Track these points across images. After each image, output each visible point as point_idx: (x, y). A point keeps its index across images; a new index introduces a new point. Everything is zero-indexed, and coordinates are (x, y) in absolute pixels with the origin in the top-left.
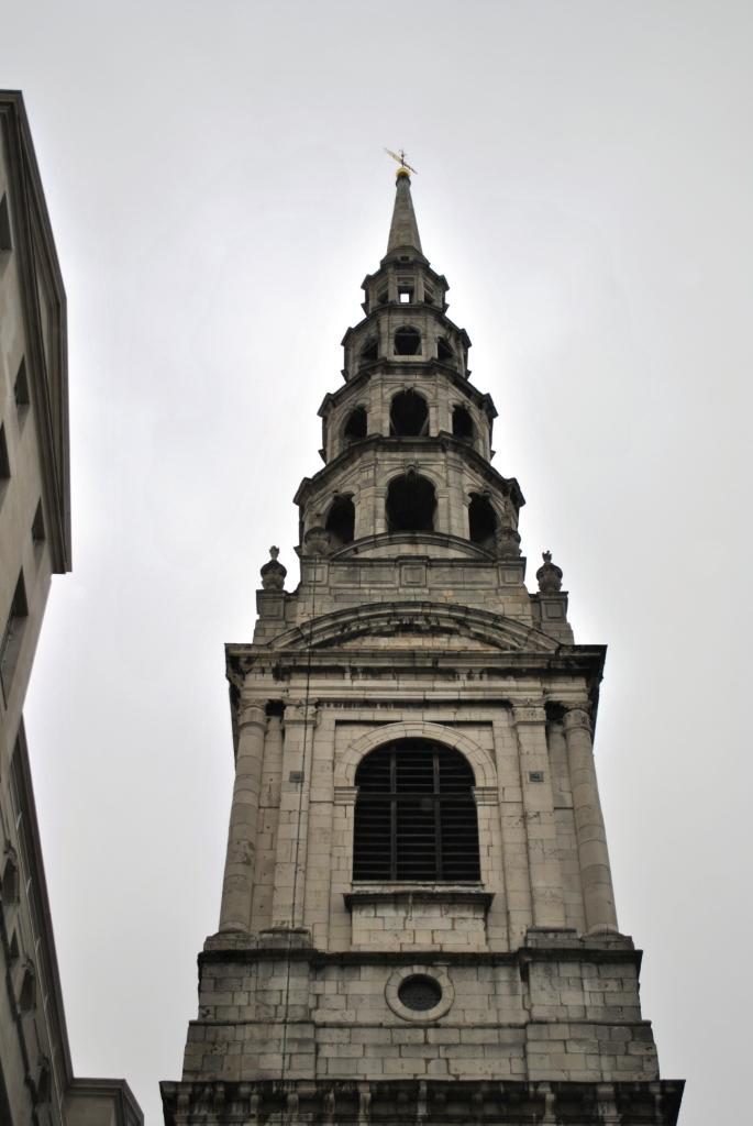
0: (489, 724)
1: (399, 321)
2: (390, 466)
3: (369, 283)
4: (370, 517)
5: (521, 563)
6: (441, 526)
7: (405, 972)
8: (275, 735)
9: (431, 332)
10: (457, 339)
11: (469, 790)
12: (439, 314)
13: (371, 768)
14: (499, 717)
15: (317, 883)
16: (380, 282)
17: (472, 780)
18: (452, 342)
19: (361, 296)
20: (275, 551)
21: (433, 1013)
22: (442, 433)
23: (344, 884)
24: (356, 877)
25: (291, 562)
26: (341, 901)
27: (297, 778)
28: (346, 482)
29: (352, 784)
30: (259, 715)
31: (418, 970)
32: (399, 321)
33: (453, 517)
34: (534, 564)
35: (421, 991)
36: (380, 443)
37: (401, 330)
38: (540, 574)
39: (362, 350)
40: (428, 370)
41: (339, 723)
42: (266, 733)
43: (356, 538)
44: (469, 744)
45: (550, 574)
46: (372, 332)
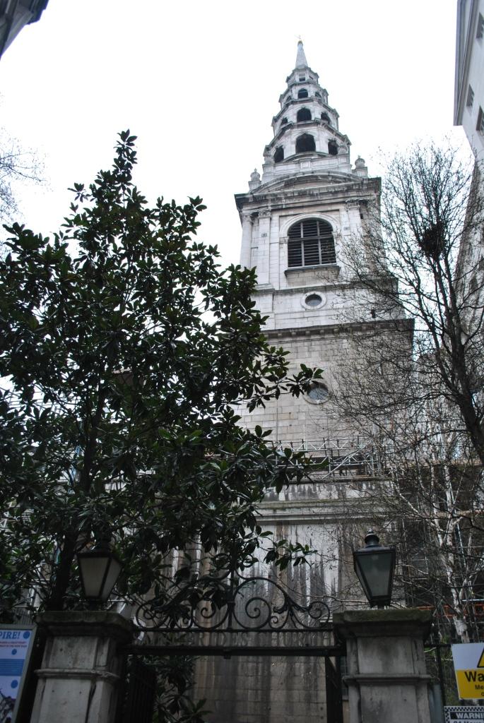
0: (338, 210)
1: (299, 88)
2: (295, 134)
3: (288, 79)
4: (290, 150)
5: (347, 156)
6: (318, 149)
7: (308, 294)
8: (255, 225)
9: (311, 91)
10: (323, 94)
11: (331, 233)
12: (316, 84)
13: (293, 231)
14: (341, 207)
15: (275, 270)
16: (292, 79)
17: (332, 230)
18: (321, 94)
20: (256, 170)
21: (319, 307)
22: (315, 118)
23: (285, 267)
24: (289, 266)
25: (261, 172)
26: (283, 275)
27: (264, 235)
29: (286, 235)
30: (249, 218)
31: (312, 293)
32: (299, 88)
33: (322, 146)
34: (353, 159)
35: (313, 299)
36: (291, 126)
37: (300, 91)
38: (356, 163)
39: (287, 101)
40: (311, 100)
41: (280, 216)
42: (252, 224)
43: (285, 158)
44: (329, 218)
46: (290, 94)
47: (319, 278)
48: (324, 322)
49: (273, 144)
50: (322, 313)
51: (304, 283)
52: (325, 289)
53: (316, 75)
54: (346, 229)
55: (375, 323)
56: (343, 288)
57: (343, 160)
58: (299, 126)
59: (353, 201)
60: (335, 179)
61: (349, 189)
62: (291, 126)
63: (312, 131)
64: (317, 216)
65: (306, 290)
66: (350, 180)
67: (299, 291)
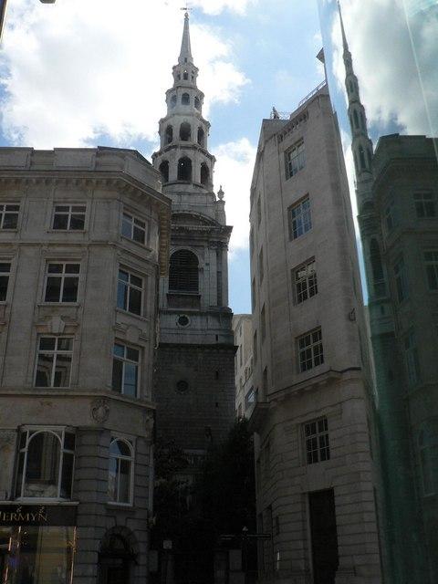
1: (183, 91)
2: (179, 154)
4: (173, 175)
7: (181, 316)
14: (205, 244)
19: (172, 71)
28: (166, 156)
34: (216, 191)
35: (183, 321)
36: (175, 147)
37: (183, 95)
44: (197, 252)
45: (221, 193)
47: (185, 305)
48: (188, 341)
49: (160, 153)
50: (189, 332)
51: (178, 307)
52: (191, 314)
53: (197, 69)
54: (207, 264)
55: (217, 345)
56: (201, 314)
57: (210, 198)
58: (182, 147)
59: (213, 242)
60: (206, 222)
61: (212, 230)
62: (175, 147)
63: (190, 154)
64: (189, 248)
65: (181, 312)
66: (213, 224)
67: (175, 313)
